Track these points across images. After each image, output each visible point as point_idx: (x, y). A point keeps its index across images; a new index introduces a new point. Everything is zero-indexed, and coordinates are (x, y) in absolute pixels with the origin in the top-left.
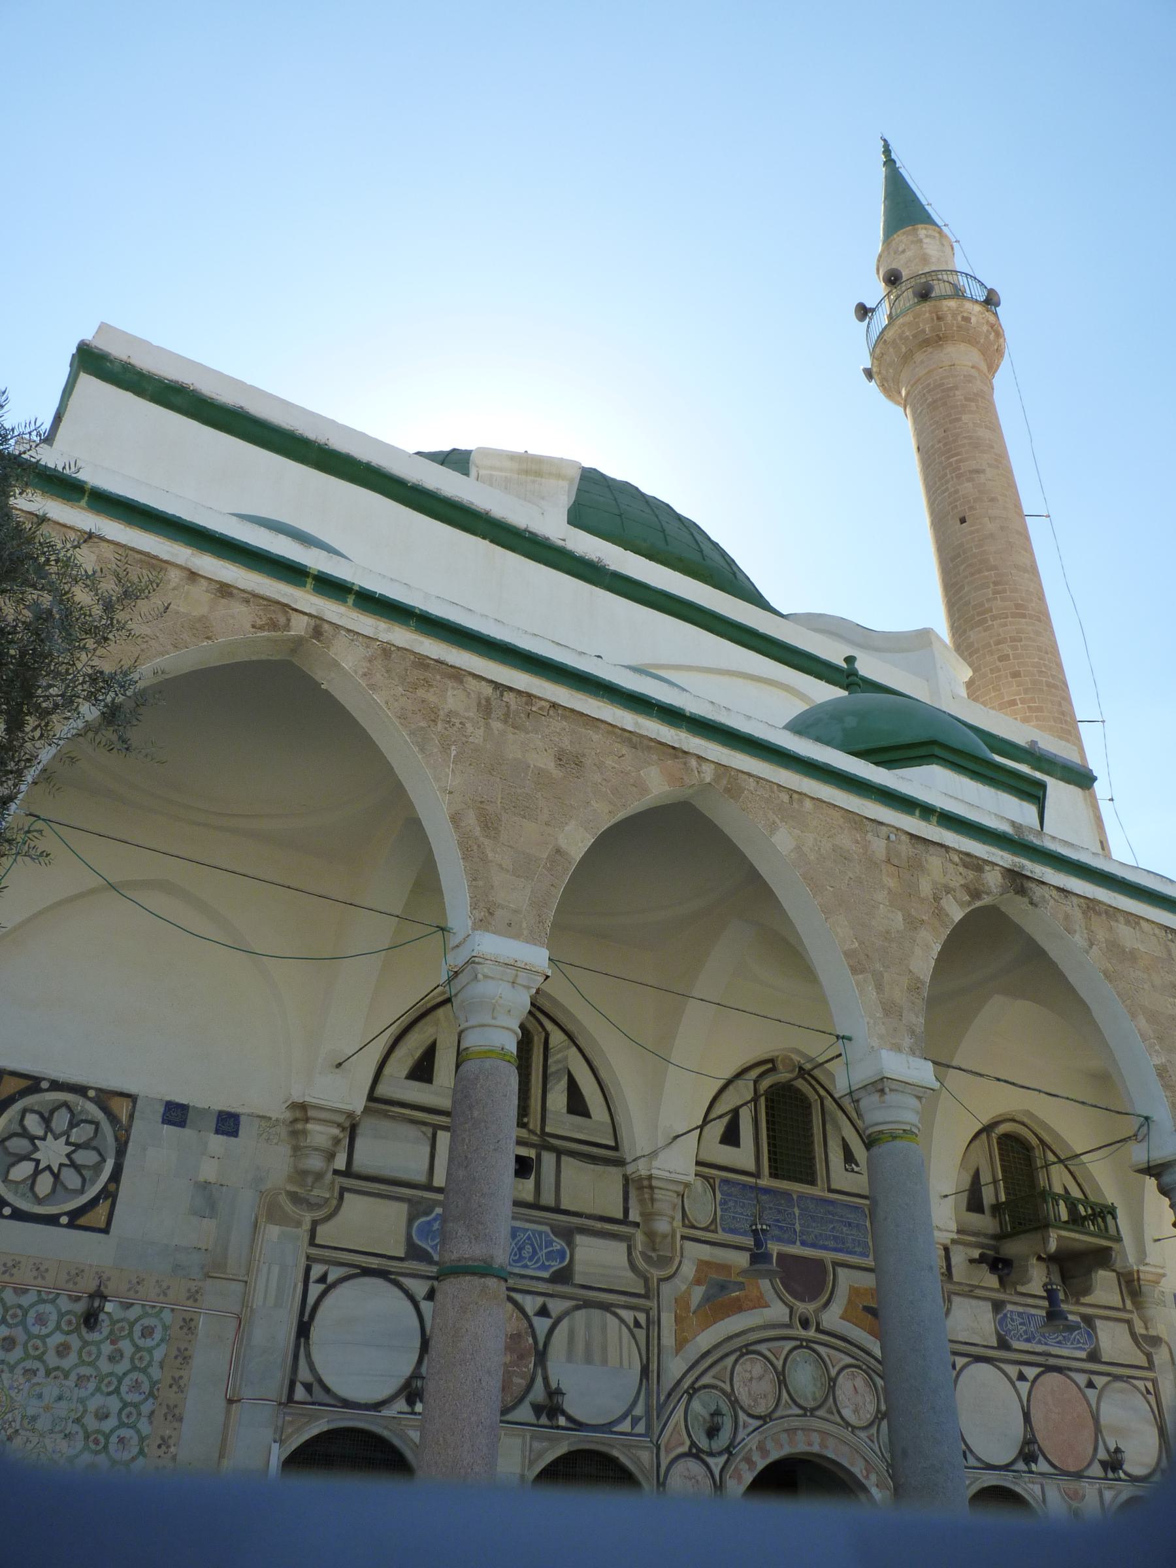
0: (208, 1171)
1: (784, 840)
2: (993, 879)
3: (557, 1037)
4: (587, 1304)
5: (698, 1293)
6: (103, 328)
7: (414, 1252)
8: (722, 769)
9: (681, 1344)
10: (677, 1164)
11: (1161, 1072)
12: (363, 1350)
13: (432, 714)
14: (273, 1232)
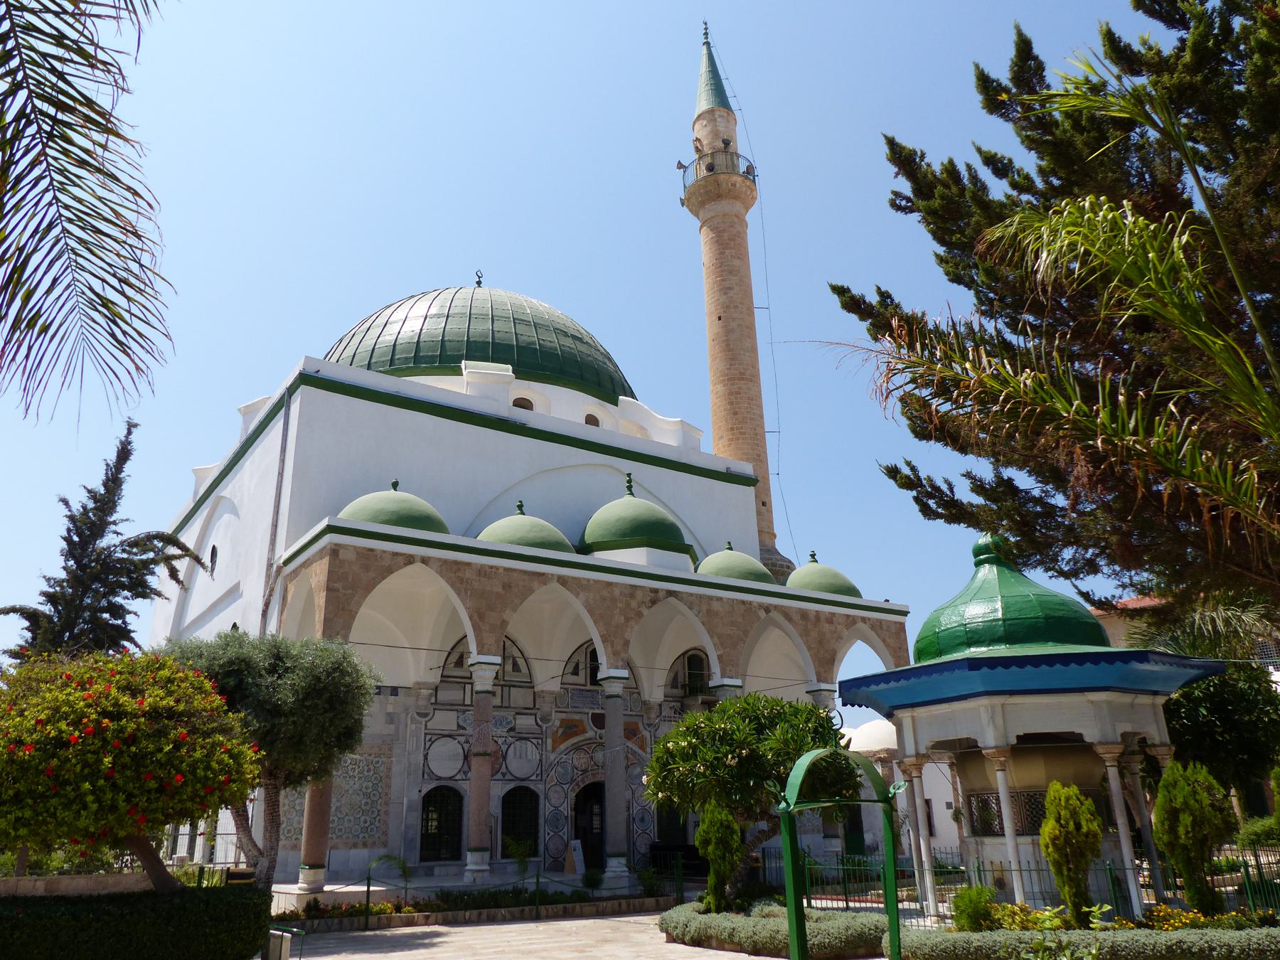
0: (390, 709)
3: (508, 643)
4: (520, 739)
5: (561, 731)
7: (459, 727)
9: (554, 750)
10: (555, 686)
11: (720, 657)
12: (445, 761)
13: (462, 581)
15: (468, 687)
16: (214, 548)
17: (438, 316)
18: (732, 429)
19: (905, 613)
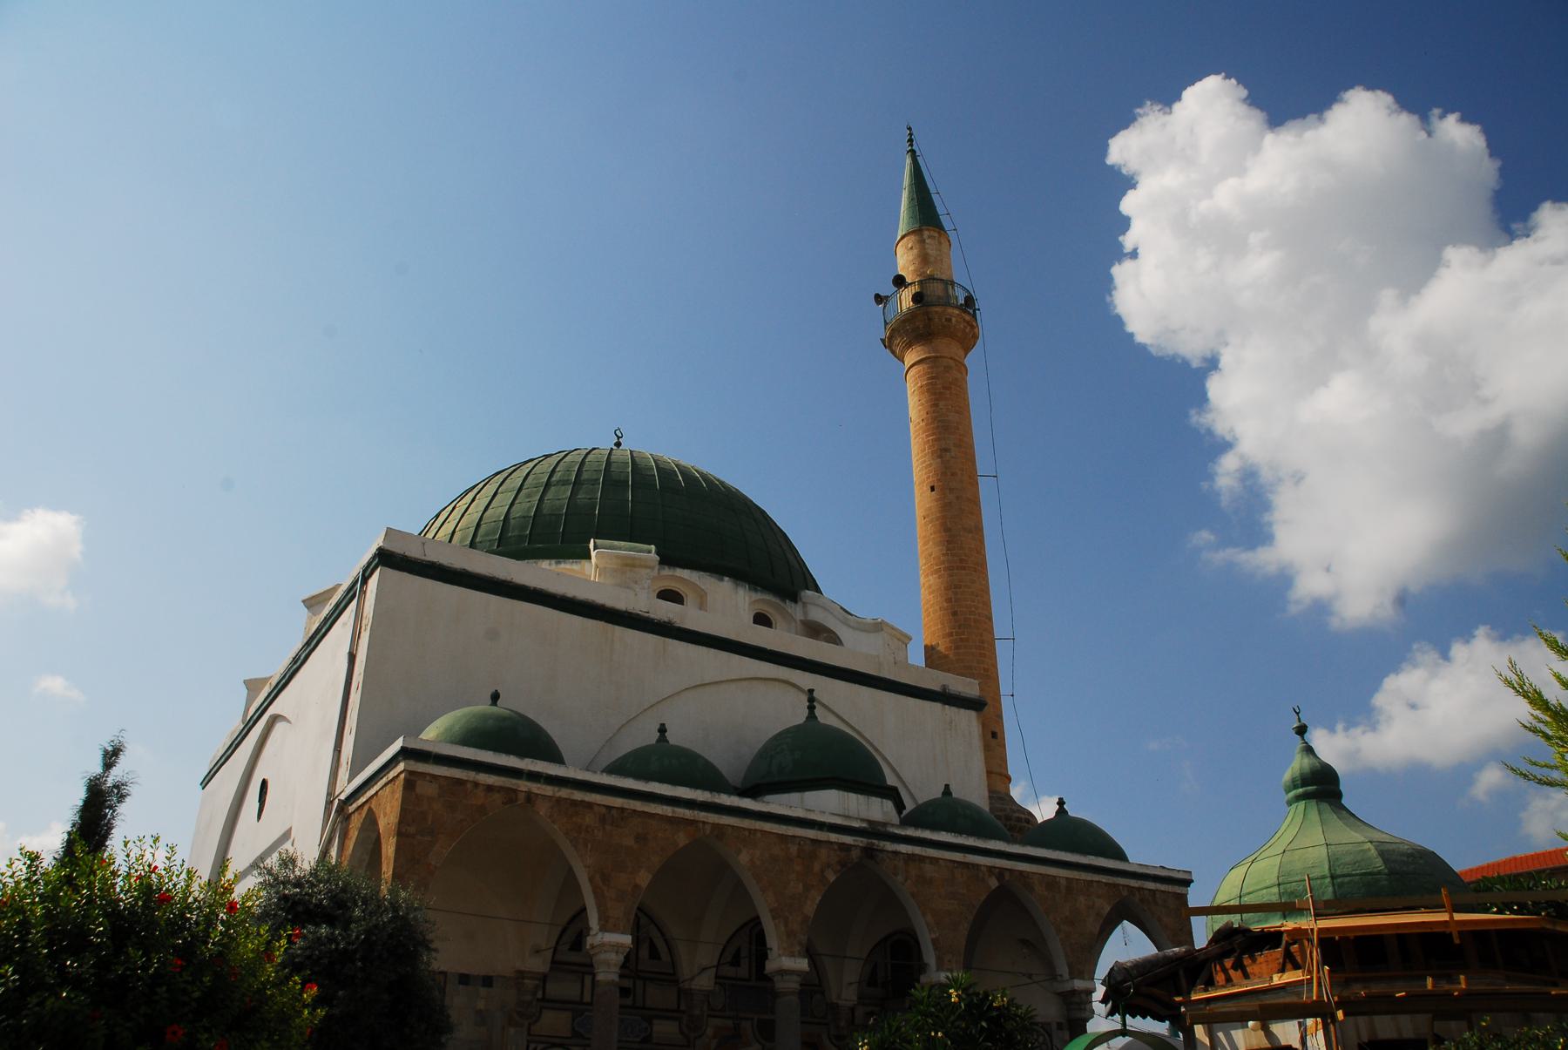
0: (481, 1005)
1: (744, 858)
2: (855, 854)
6: (390, 532)
8: (716, 826)
10: (705, 982)
11: (935, 942)
14: (512, 1030)
15: (588, 979)
16: (264, 784)
17: (564, 483)
18: (951, 634)
19: (1187, 883)
